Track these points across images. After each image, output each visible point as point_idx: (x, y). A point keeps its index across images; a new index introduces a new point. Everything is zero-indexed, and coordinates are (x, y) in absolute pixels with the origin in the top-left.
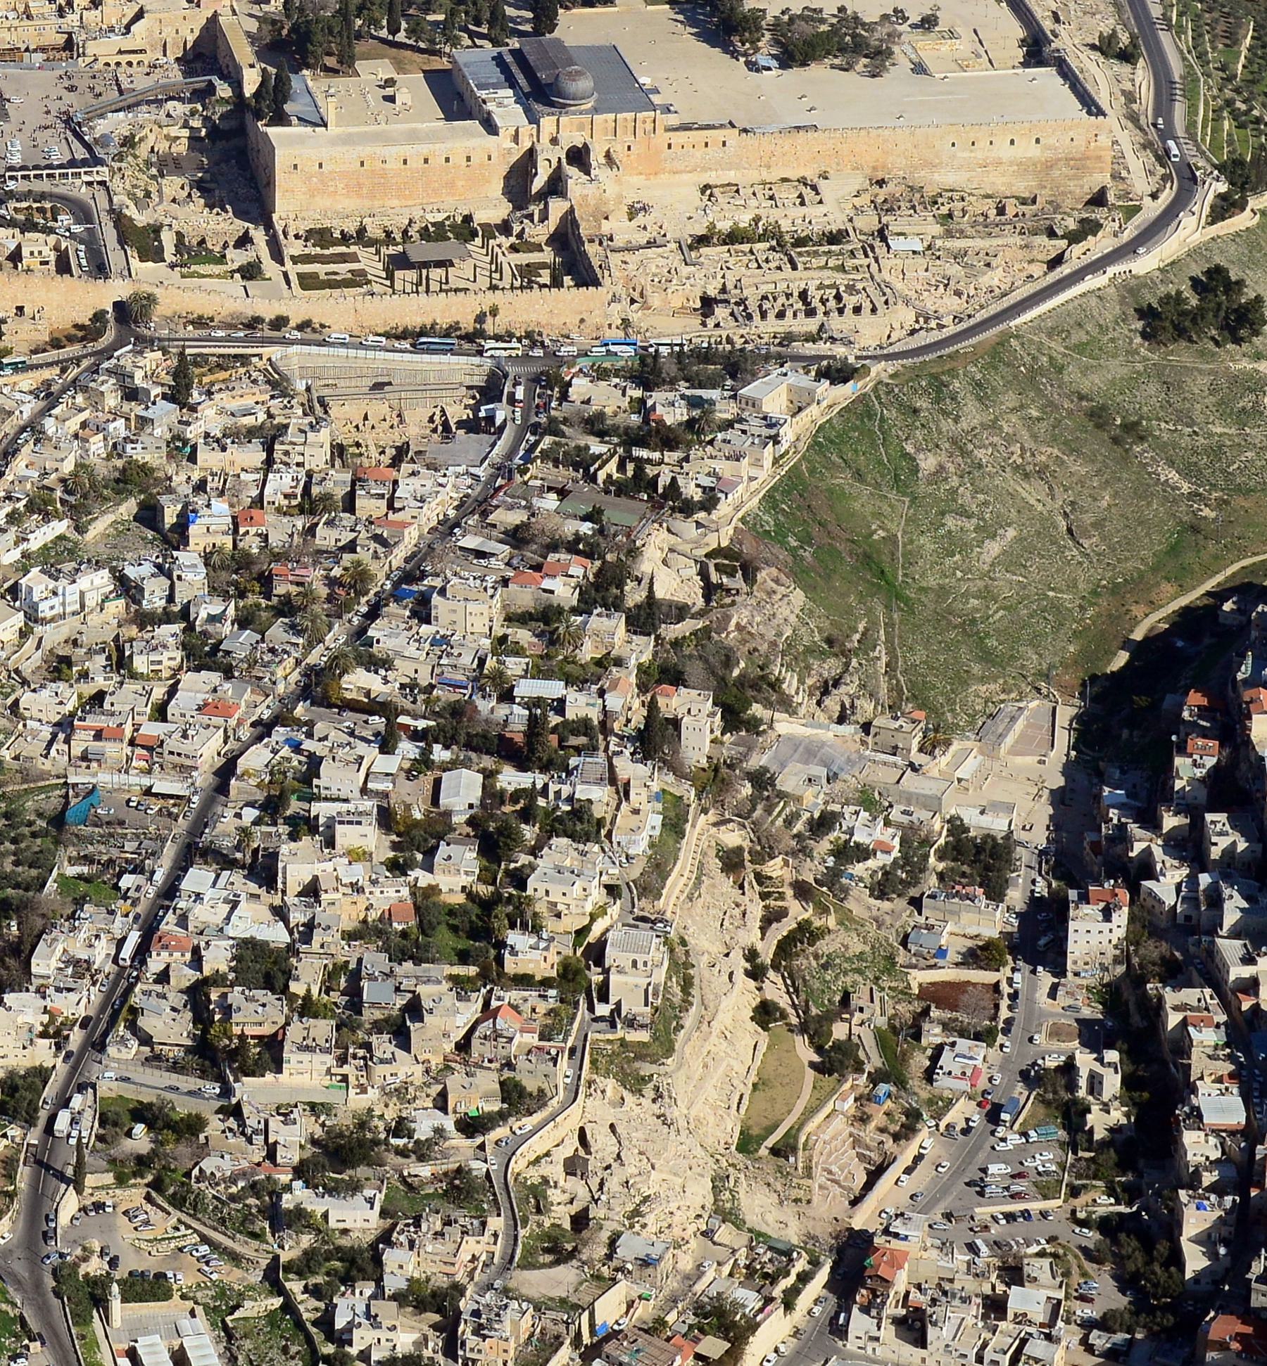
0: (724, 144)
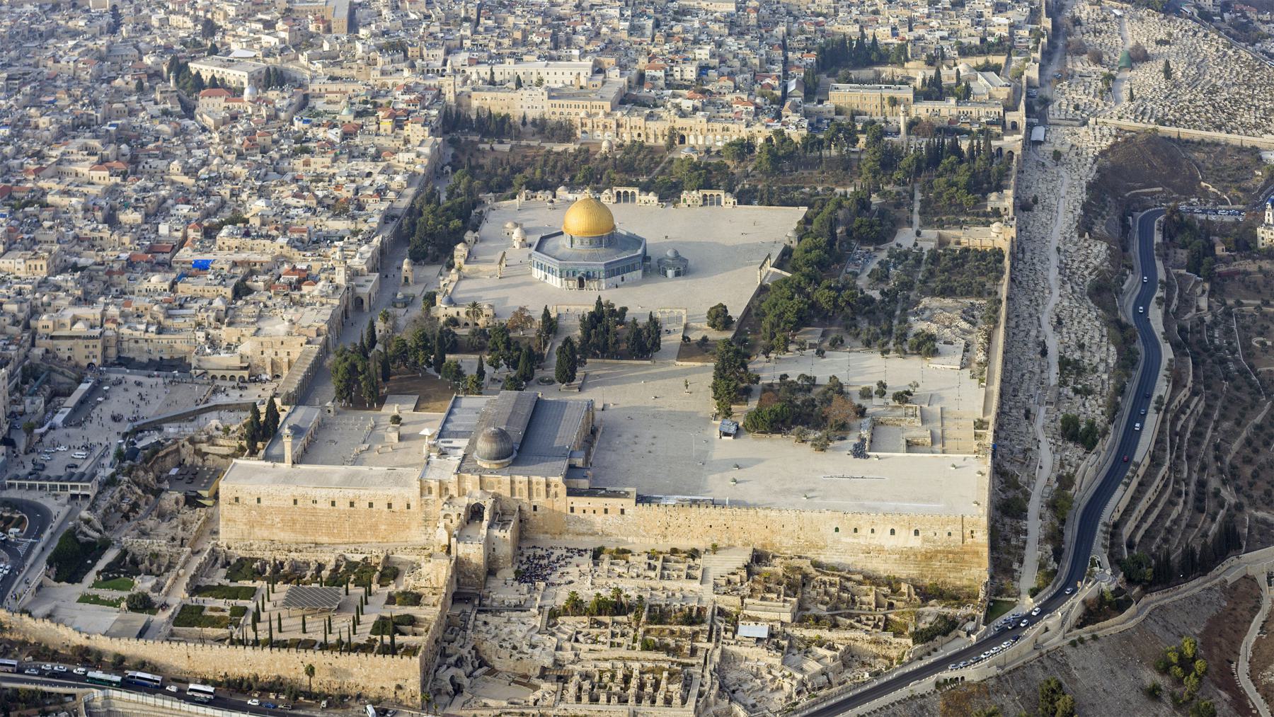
0: (622, 511)
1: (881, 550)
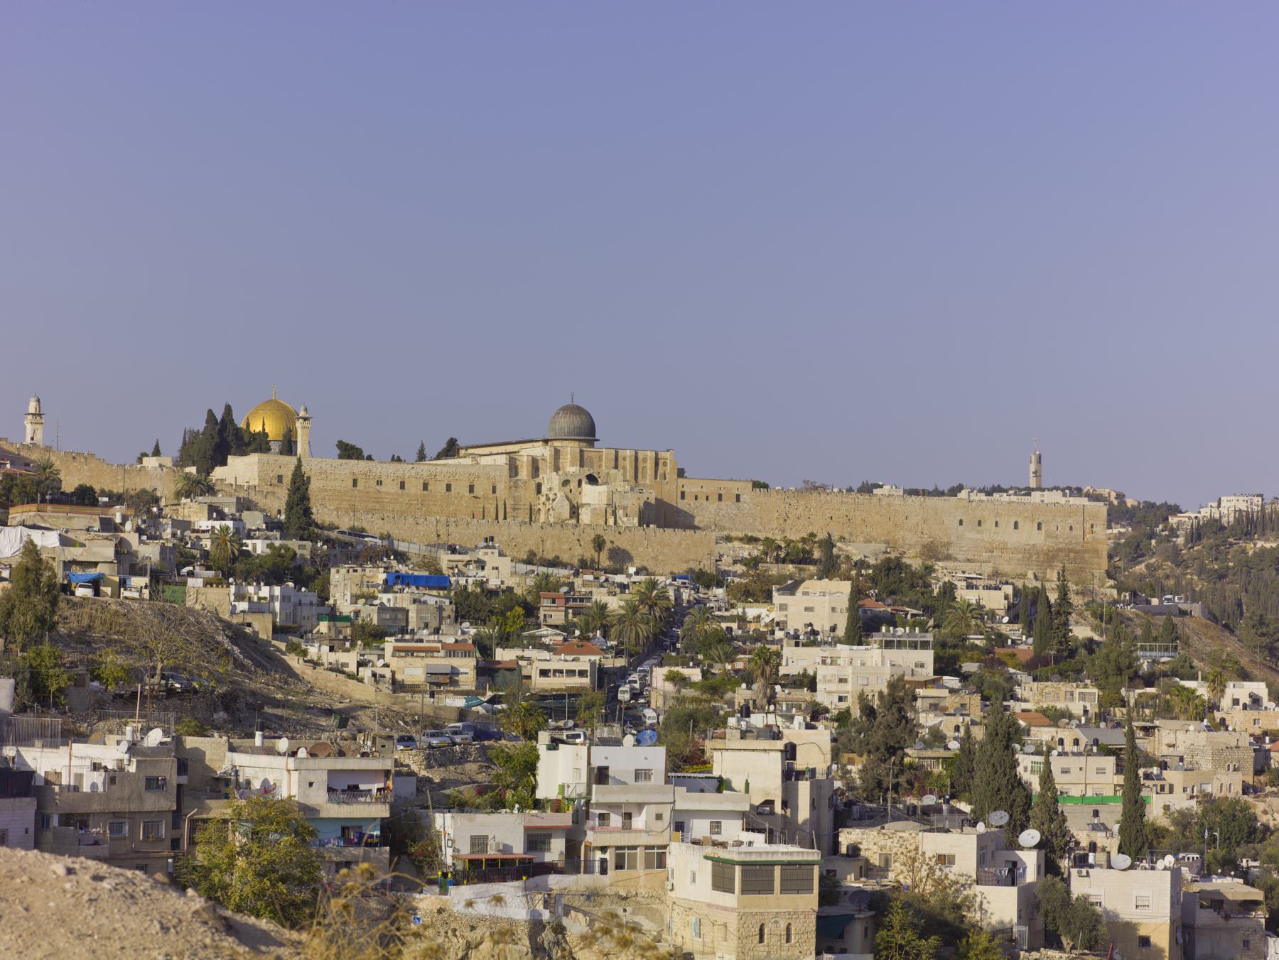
0: (738, 498)
1: (1004, 548)
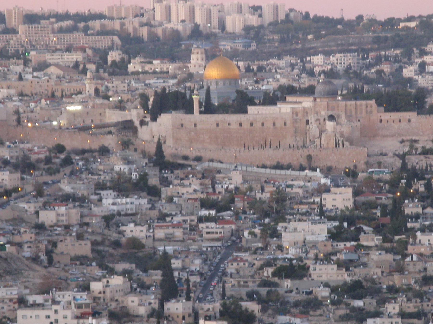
0: (409, 121)
